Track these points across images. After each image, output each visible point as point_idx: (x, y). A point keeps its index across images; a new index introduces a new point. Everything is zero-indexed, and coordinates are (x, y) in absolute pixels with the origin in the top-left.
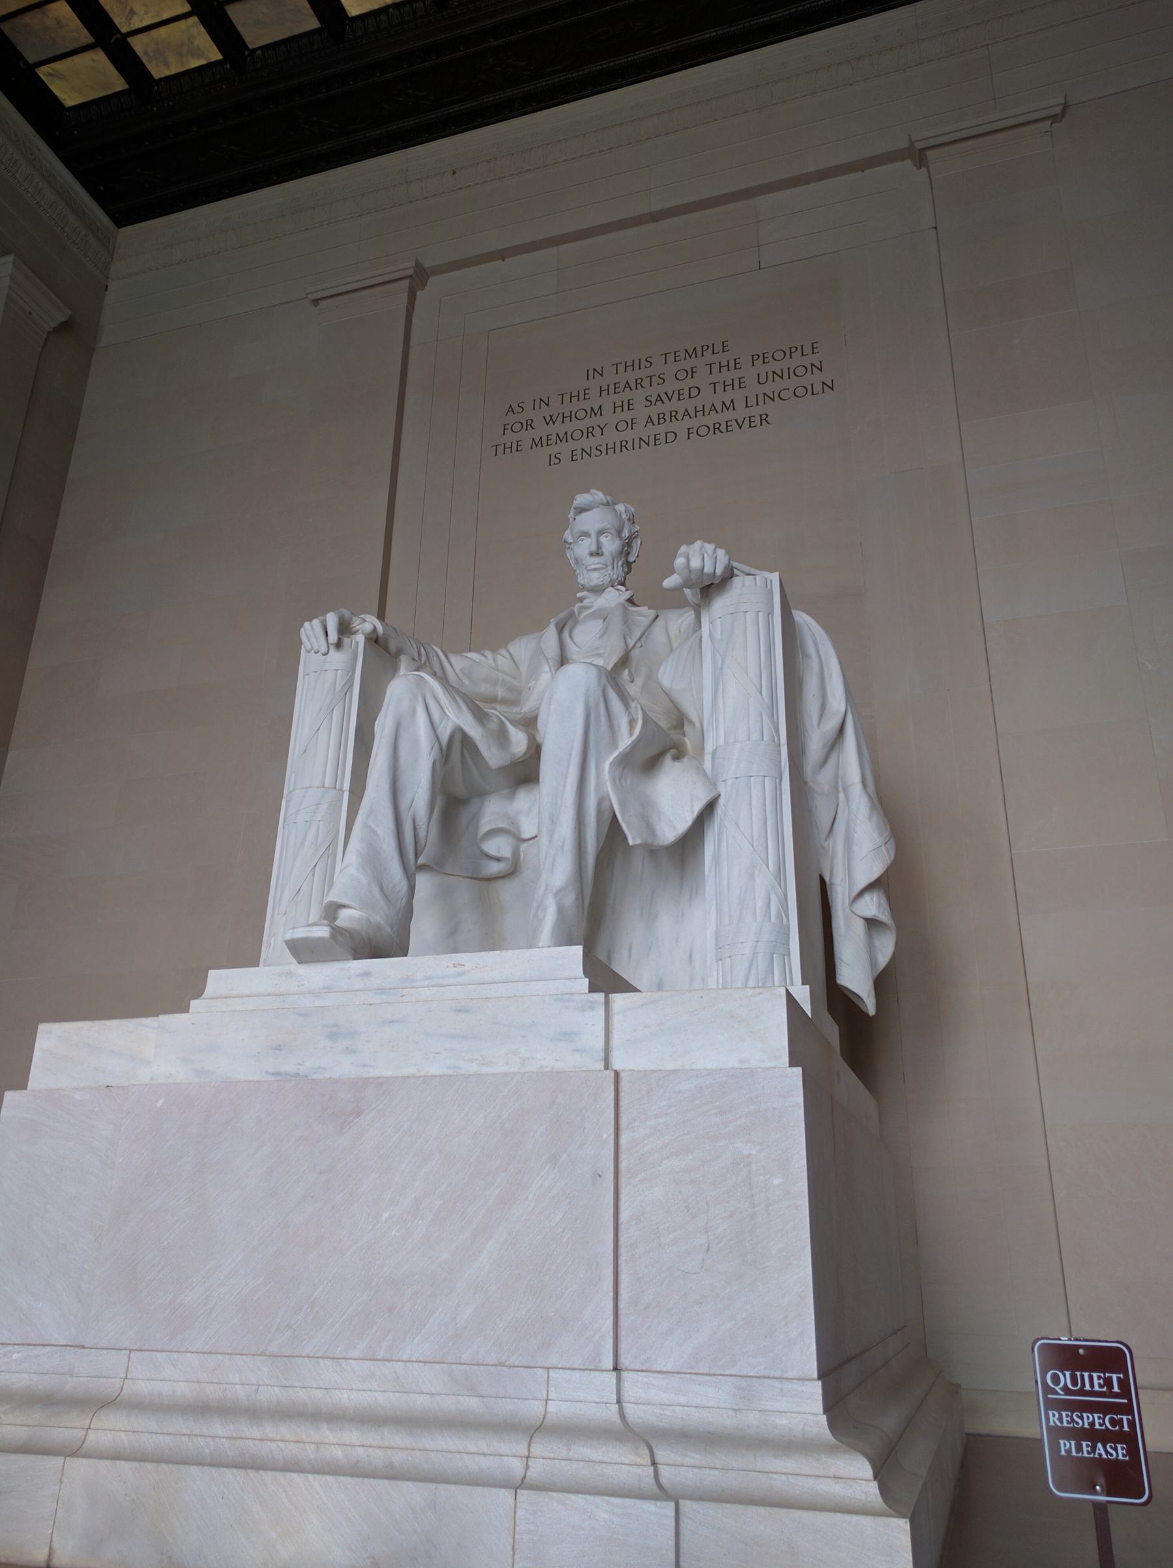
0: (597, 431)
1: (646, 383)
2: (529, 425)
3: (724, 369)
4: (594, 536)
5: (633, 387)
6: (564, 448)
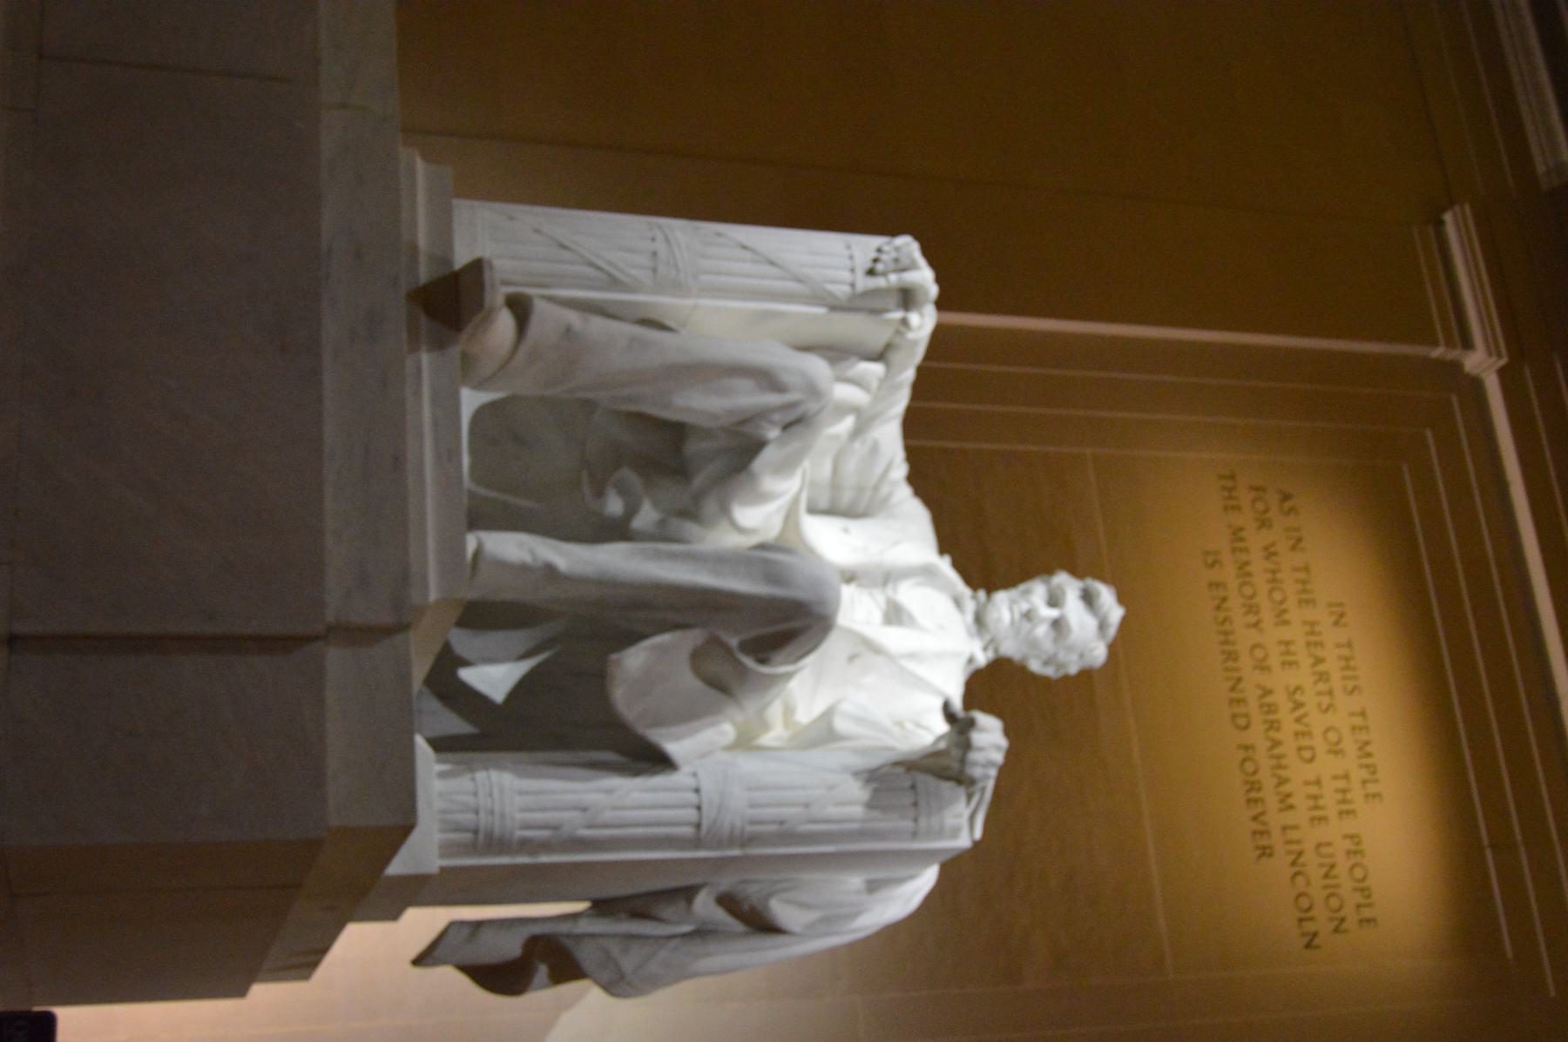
0: (1252, 619)
1: (1322, 686)
2: (1264, 523)
3: (1339, 796)
4: (1053, 613)
5: (1321, 668)
6: (1228, 573)
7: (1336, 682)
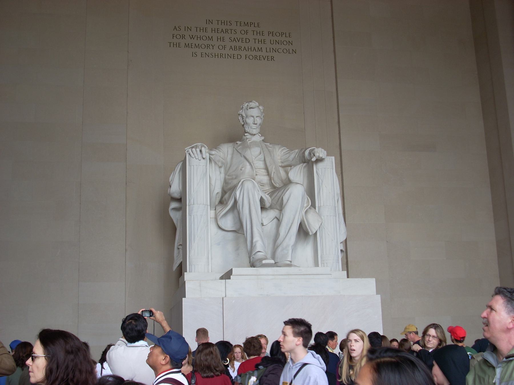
1: (229, 31)
5: (225, 32)
6: (199, 51)
7: (228, 27)
